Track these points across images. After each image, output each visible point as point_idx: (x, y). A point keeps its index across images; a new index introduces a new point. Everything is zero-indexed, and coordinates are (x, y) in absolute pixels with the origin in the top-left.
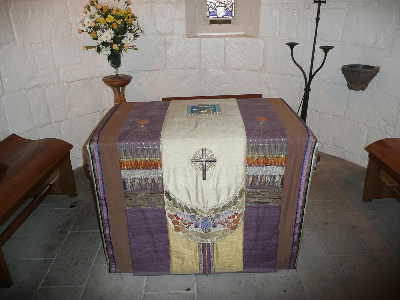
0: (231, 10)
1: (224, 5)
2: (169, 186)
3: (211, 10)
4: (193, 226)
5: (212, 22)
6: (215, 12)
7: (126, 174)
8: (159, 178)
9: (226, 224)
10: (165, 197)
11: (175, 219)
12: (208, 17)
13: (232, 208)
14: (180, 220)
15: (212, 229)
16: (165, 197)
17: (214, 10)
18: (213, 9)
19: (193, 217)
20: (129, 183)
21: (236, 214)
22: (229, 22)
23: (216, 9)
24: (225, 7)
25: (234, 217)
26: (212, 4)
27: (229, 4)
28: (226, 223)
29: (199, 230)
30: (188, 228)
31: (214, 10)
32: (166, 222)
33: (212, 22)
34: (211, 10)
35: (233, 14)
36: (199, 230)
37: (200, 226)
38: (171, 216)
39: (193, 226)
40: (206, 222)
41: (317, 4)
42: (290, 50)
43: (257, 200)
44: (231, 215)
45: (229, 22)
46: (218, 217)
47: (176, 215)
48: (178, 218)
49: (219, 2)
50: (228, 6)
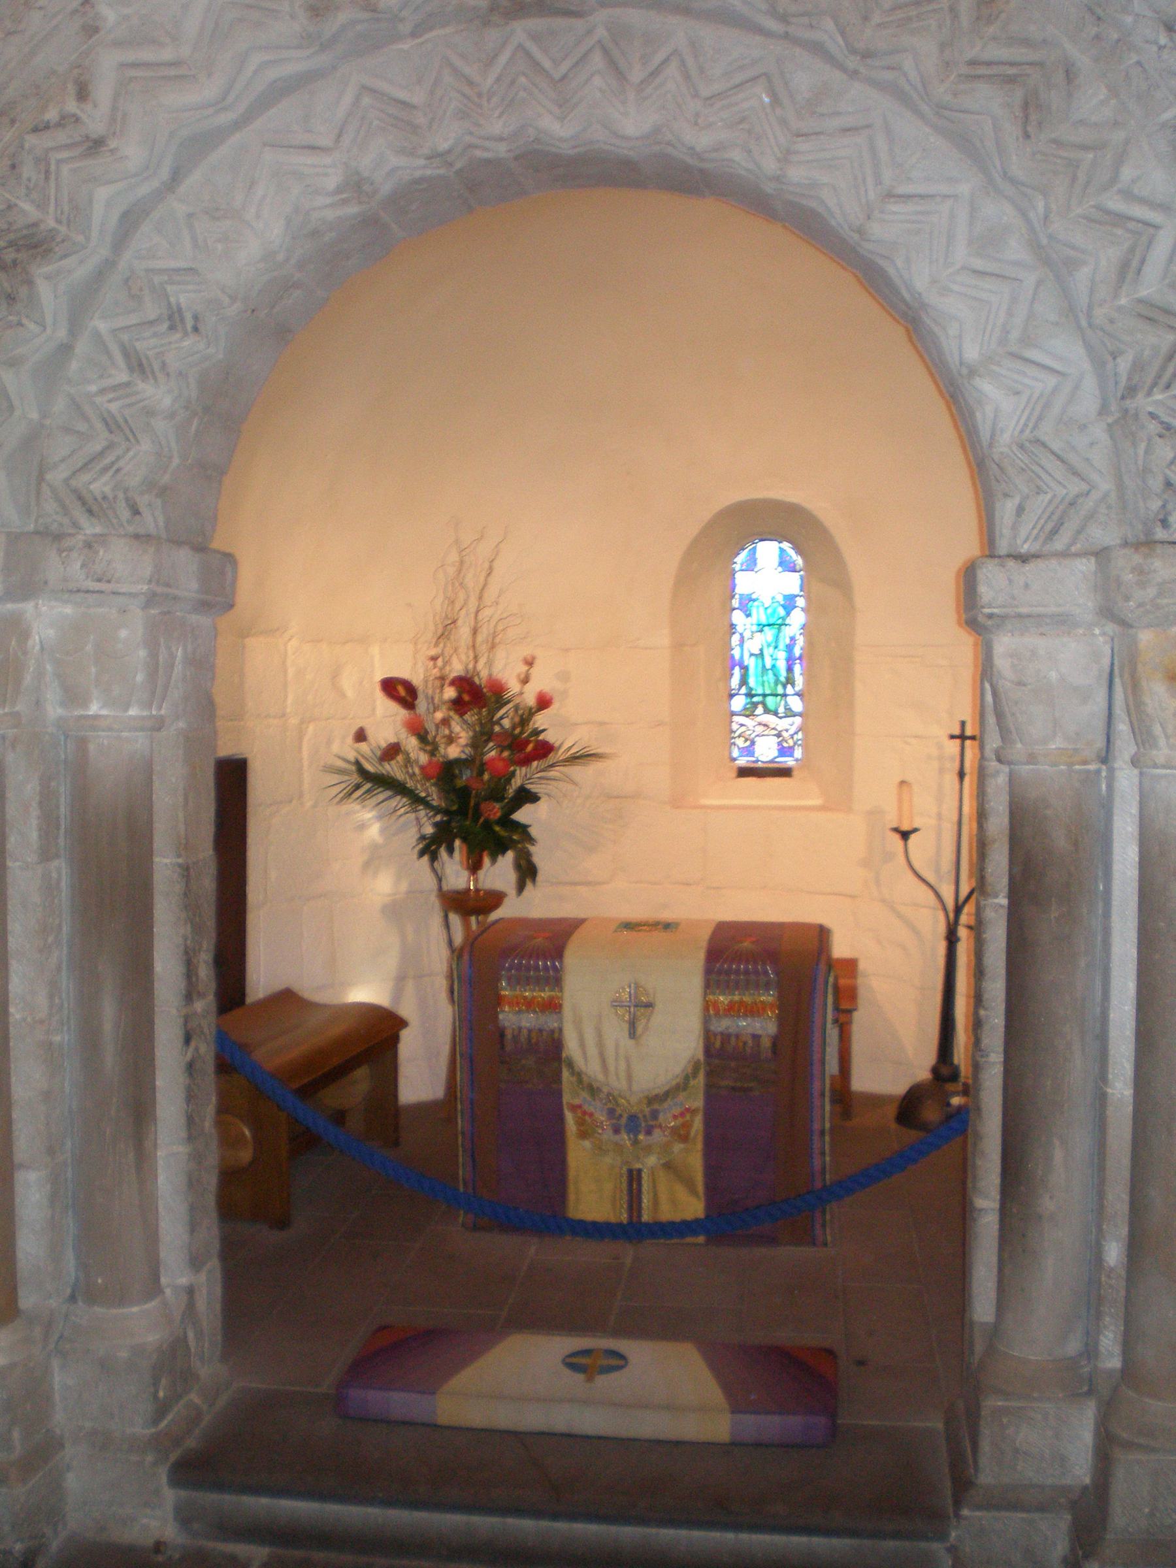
0: (795, 743)
1: (775, 732)
3: (740, 742)
5: (744, 772)
6: (749, 751)
12: (735, 759)
17: (748, 743)
18: (746, 740)
22: (785, 772)
23: (753, 743)
24: (779, 735)
26: (743, 729)
31: (748, 743)
33: (744, 772)
34: (740, 742)
35: (798, 753)
41: (958, 741)
45: (785, 772)
49: (765, 725)
50: (785, 734)
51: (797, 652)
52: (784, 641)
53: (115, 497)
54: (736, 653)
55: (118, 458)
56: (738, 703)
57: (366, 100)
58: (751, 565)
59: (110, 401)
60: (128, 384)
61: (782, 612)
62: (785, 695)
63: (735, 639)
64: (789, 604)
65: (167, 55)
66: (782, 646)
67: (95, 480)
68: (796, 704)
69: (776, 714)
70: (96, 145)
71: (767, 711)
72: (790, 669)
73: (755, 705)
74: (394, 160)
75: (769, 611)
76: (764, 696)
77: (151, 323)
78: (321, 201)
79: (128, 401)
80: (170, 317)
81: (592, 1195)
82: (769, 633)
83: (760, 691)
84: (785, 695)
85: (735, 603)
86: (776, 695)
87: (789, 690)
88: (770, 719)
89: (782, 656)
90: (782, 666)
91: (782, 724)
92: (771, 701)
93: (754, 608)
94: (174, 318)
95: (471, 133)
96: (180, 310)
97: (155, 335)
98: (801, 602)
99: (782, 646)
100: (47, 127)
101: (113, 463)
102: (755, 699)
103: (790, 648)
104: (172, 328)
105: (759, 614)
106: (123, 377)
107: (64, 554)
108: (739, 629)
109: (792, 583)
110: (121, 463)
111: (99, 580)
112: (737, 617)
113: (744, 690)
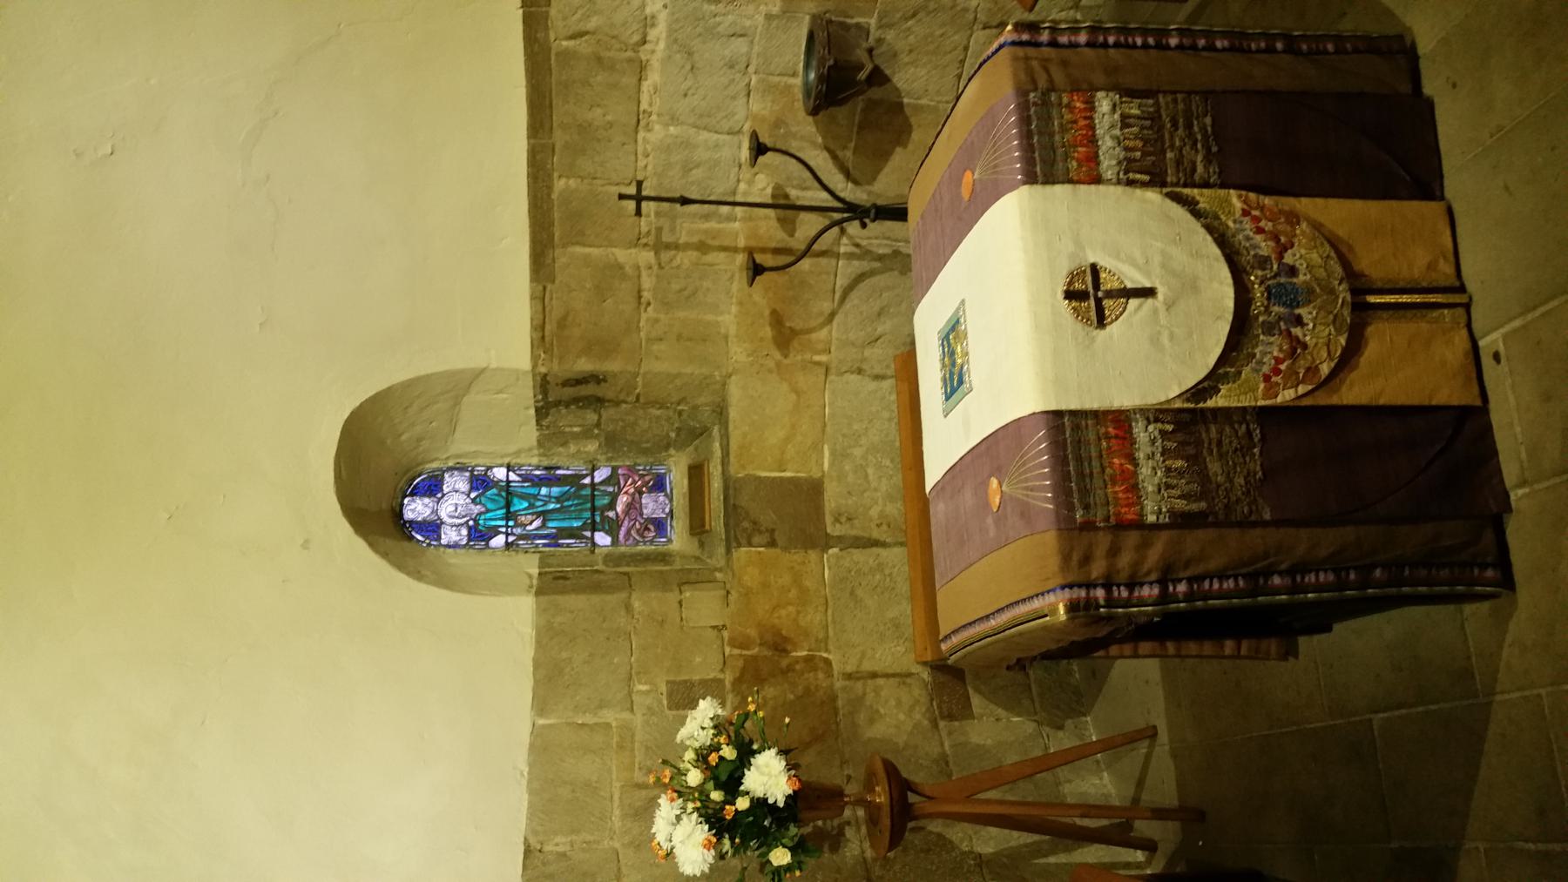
2: (1168, 382)
4: (1297, 331)
8: (1157, 420)
9: (1283, 239)
10: (1210, 403)
13: (1231, 224)
14: (1283, 367)
15: (1301, 277)
16: (1210, 403)
18: (647, 529)
19: (1269, 329)
21: (1245, 213)
24: (641, 493)
25: (1256, 220)
27: (634, 482)
28: (1277, 240)
30: (1305, 346)
37: (1297, 311)
39: (1297, 331)
42: (766, 275)
44: (1248, 225)
46: (1263, 262)
48: (1277, 371)
58: (432, 528)
61: (494, 491)
62: (593, 485)
64: (480, 482)
66: (533, 491)
71: (612, 506)
73: (603, 518)
75: (490, 506)
76: (593, 509)
82: (519, 505)
83: (588, 514)
84: (593, 485)
86: (593, 496)
88: (622, 501)
89: (544, 491)
90: (556, 491)
92: (602, 501)
99: (533, 491)
102: (598, 519)
108: (511, 539)
109: (456, 484)
113: (588, 534)
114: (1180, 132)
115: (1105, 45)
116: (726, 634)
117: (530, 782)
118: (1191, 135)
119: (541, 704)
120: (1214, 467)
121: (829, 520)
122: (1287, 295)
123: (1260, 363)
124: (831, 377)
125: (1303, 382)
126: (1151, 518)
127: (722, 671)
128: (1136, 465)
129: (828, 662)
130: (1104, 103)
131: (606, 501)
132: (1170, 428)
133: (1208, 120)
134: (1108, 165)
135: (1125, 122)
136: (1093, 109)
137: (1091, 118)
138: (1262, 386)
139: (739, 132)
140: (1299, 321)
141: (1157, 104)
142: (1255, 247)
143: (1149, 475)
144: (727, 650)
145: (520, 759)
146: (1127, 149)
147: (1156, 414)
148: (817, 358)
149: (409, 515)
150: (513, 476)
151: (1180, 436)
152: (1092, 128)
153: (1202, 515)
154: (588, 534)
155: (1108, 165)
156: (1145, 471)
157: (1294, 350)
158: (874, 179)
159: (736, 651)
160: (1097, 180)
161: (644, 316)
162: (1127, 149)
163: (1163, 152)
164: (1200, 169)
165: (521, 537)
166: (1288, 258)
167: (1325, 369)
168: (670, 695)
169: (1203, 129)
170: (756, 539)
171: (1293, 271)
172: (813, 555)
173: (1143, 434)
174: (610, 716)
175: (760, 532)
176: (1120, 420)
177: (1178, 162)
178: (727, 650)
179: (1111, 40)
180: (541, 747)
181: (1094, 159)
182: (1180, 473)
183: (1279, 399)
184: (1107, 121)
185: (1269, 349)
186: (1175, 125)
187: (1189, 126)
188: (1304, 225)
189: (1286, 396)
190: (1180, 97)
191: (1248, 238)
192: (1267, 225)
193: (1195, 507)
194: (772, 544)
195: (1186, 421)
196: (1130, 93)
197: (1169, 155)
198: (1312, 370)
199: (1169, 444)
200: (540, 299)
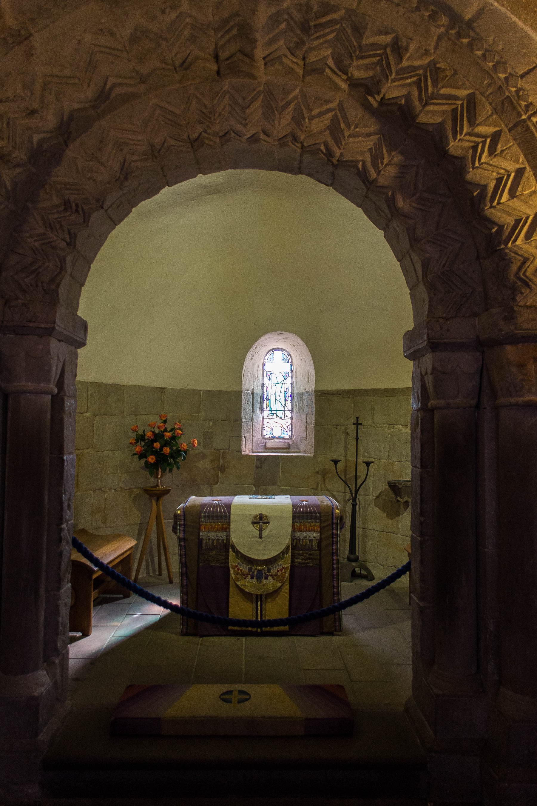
2: (234, 539)
3: (267, 429)
7: (203, 534)
9: (275, 577)
11: (236, 569)
14: (239, 571)
19: (250, 570)
20: (204, 542)
29: (254, 581)
30: (245, 578)
32: (229, 571)
36: (254, 581)
38: (234, 568)
39: (249, 577)
40: (260, 568)
43: (300, 560)
46: (269, 570)
47: (237, 566)
48: (238, 569)
51: (289, 394)
52: (283, 390)
53: (37, 286)
54: (265, 394)
55: (39, 267)
56: (266, 413)
57: (158, 111)
59: (35, 241)
60: (45, 234)
62: (284, 411)
63: (265, 388)
65: (67, 72)
67: (27, 277)
68: (289, 414)
69: (281, 418)
70: (32, 113)
72: (286, 400)
74: (171, 142)
76: (276, 411)
77: (57, 206)
78: (135, 158)
79: (43, 242)
80: (65, 204)
81: (239, 609)
82: (279, 386)
85: (265, 375)
87: (286, 409)
88: (279, 420)
91: (283, 422)
92: (279, 413)
93: (273, 376)
94: (67, 204)
95: (205, 132)
96: (69, 202)
97: (58, 212)
98: (290, 374)
100: (8, 100)
101: (37, 269)
103: (286, 392)
104: (65, 210)
105: (274, 380)
106: (41, 230)
107: (12, 309)
108: (267, 385)
110: (40, 270)
111: (30, 321)
112: (266, 380)
113: (268, 409)
114: (308, 556)
115: (333, 538)
116: (227, 450)
117: (183, 389)
118: (307, 559)
119: (208, 393)
120: (214, 552)
121: (264, 487)
122: (260, 576)
123: (241, 565)
124: (313, 491)
125: (235, 576)
126: (201, 534)
127: (215, 449)
128: (215, 532)
129: (217, 483)
130: (315, 535)
131: (279, 415)
132: (225, 542)
133: (311, 565)
134: (298, 534)
135: (311, 540)
136: (315, 531)
137: (312, 531)
138: (234, 564)
139: (389, 459)
140: (252, 578)
141: (316, 550)
142: (273, 568)
143: (212, 535)
144: (222, 451)
145: (191, 386)
146: (303, 540)
147: (228, 538)
148: (319, 486)
149: (276, 352)
150: (288, 385)
151: (222, 544)
152: (309, 531)
153: (202, 547)
154: (268, 409)
155: (298, 534)
156: (214, 534)
157: (244, 575)
158: (377, 506)
159: (221, 454)
160: (294, 530)
161: (333, 427)
162: (303, 540)
163: (302, 550)
164: (297, 560)
165: (267, 387)
166: (270, 578)
167: (239, 583)
168: (208, 432)
169: (309, 563)
170: (258, 462)
171: (266, 578)
172: (253, 481)
173: (223, 534)
174: (203, 413)
175: (261, 464)
176: (226, 529)
177: (299, 554)
178: (222, 451)
179: (334, 539)
180: (195, 392)
181: (300, 530)
182: (213, 543)
183: (231, 569)
184: (312, 535)
185: (244, 568)
186: (310, 555)
187: (309, 559)
188: (279, 585)
189: (232, 571)
190: (318, 557)
191: (276, 567)
192: (279, 573)
193: (204, 545)
194: (257, 467)
195: (226, 546)
196: (320, 542)
197: (301, 552)
198: (238, 580)
199: (220, 541)
200: (338, 393)
